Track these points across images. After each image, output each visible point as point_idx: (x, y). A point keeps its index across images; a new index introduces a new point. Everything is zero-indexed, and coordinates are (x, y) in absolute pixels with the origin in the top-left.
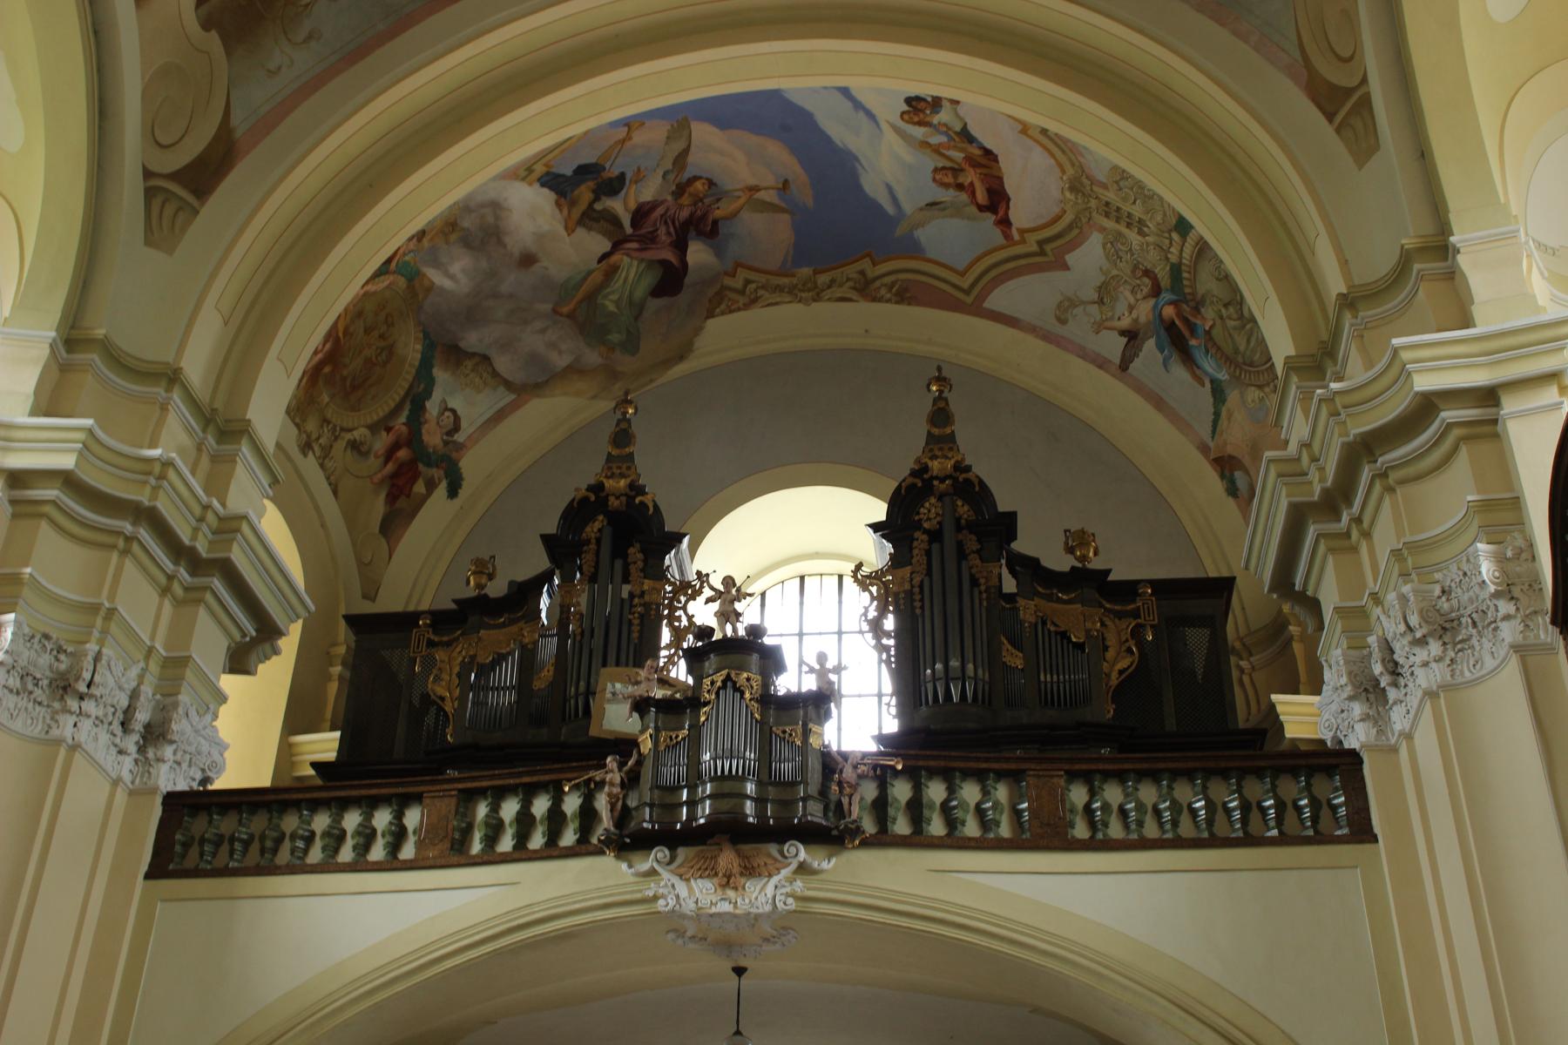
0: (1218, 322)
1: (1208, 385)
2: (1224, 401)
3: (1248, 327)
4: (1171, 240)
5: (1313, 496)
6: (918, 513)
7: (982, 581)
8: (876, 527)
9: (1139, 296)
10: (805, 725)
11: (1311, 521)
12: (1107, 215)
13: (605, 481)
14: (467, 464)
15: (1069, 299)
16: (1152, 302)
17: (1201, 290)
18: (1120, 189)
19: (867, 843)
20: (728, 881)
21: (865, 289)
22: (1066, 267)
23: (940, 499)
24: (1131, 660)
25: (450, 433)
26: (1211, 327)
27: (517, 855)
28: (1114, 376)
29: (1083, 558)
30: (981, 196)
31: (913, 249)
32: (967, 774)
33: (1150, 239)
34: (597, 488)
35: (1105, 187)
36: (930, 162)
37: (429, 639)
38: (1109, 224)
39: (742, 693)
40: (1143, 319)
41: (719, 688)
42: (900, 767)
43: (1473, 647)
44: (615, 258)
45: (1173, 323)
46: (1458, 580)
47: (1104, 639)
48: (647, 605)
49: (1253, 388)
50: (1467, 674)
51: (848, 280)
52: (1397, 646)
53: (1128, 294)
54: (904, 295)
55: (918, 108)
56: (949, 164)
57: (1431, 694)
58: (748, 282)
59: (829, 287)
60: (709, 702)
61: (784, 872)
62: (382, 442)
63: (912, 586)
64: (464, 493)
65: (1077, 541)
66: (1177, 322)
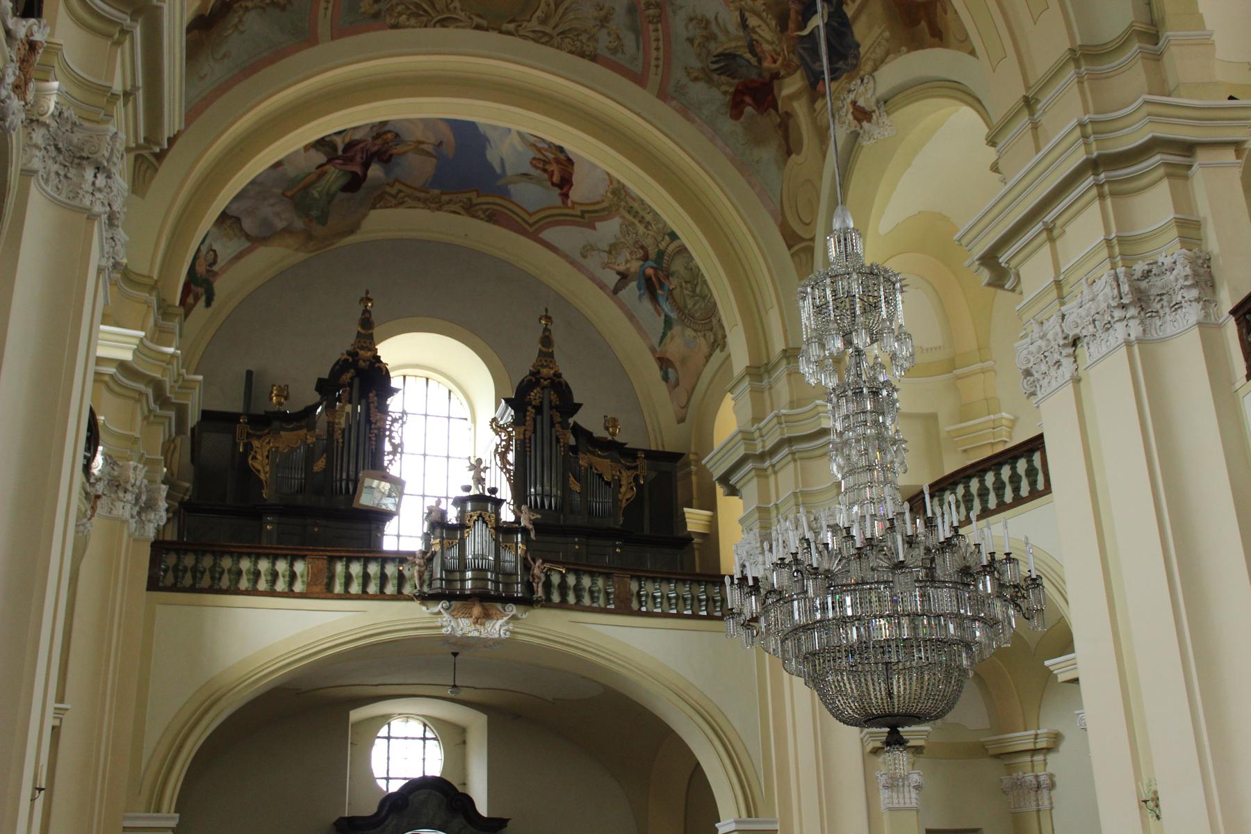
0: (678, 289)
1: (663, 317)
2: (671, 328)
3: (697, 298)
4: (663, 238)
7: (561, 440)
12: (629, 212)
13: (358, 350)
14: (219, 286)
15: (591, 245)
16: (641, 263)
19: (543, 606)
21: (470, 209)
22: (594, 228)
23: (543, 388)
26: (673, 289)
28: (608, 295)
29: (613, 434)
30: (556, 178)
31: (504, 193)
32: (585, 572)
33: (650, 233)
36: (532, 154)
37: (247, 432)
38: (630, 217)
40: (632, 270)
45: (650, 278)
47: (620, 480)
51: (460, 201)
53: (628, 254)
54: (493, 217)
56: (542, 157)
58: (400, 191)
59: (448, 203)
64: (215, 304)
65: (611, 423)
66: (653, 279)
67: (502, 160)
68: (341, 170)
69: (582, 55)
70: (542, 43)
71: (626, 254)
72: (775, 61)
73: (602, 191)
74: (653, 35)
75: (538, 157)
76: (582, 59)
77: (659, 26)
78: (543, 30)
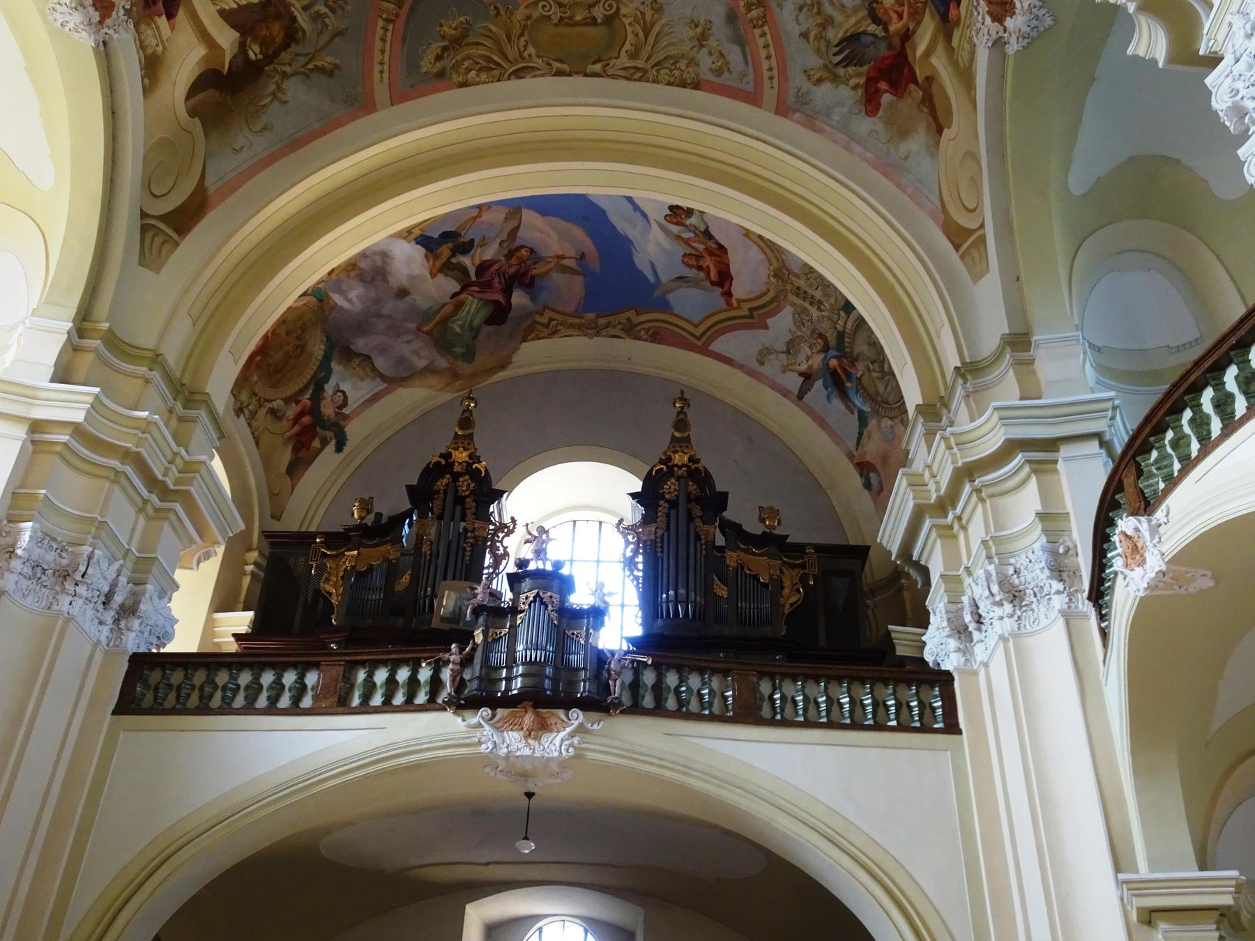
0: (867, 373)
1: (856, 414)
2: (866, 425)
3: (887, 378)
4: (839, 316)
5: (930, 499)
6: (663, 488)
7: (703, 537)
8: (634, 496)
9: (814, 350)
10: (587, 630)
11: (928, 516)
12: (798, 295)
13: (453, 452)
15: (767, 349)
16: (822, 356)
17: (857, 350)
18: (808, 279)
20: (530, 734)
21: (630, 331)
22: (767, 328)
24: (798, 597)
25: (340, 407)
26: (861, 376)
27: (385, 708)
30: (713, 275)
31: (664, 306)
32: (692, 669)
34: (447, 456)
35: (798, 276)
36: (681, 250)
38: (799, 301)
39: (546, 606)
40: (815, 366)
41: (531, 602)
42: (650, 662)
43: (1033, 610)
44: (463, 296)
45: (835, 370)
46: (1025, 564)
47: (782, 582)
48: (476, 538)
49: (887, 419)
50: (1028, 627)
51: (619, 323)
52: (981, 604)
53: (807, 349)
54: (656, 337)
55: (677, 214)
56: (694, 252)
57: (1003, 638)
58: (551, 320)
59: (606, 327)
60: (524, 611)
61: (568, 730)
62: (293, 410)
63: (656, 537)
64: (346, 449)
66: (839, 370)
67: (652, 264)
68: (480, 299)
69: (683, 84)
70: (635, 80)
71: (805, 350)
72: (901, 17)
73: (765, 279)
74: (761, 42)
75: (688, 252)
76: (684, 90)
77: (766, 28)
78: (634, 64)
